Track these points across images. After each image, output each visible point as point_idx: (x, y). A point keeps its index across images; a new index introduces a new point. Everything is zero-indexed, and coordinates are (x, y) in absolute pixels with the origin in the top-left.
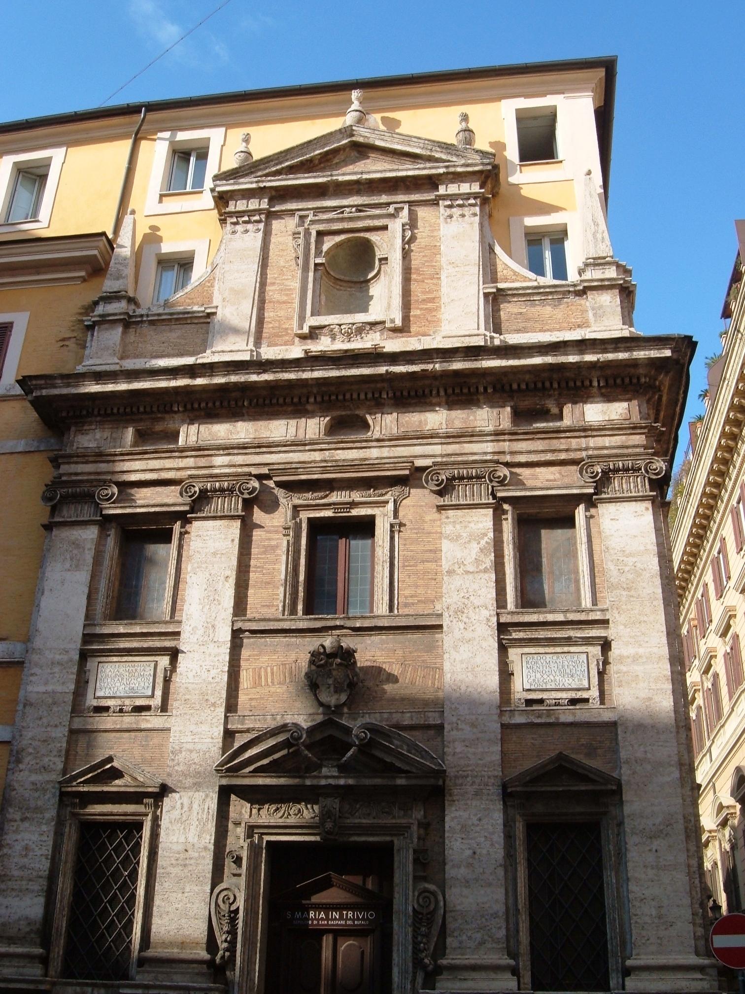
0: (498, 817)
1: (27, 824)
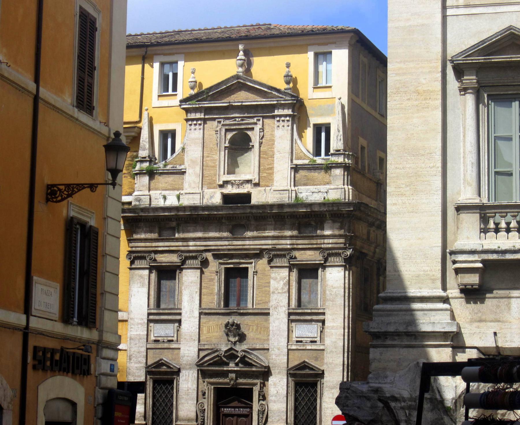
0: (285, 380)
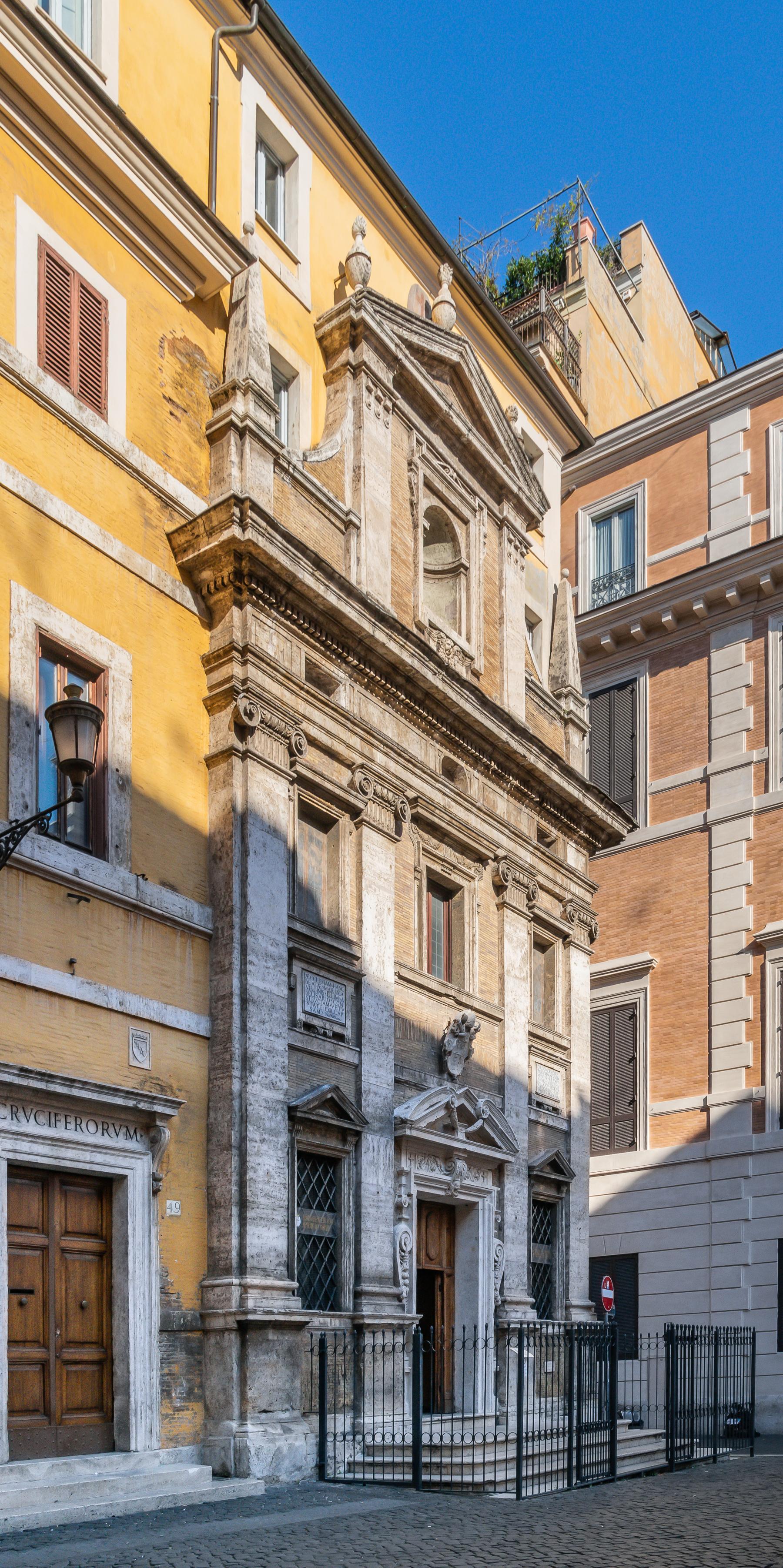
1: (265, 1147)
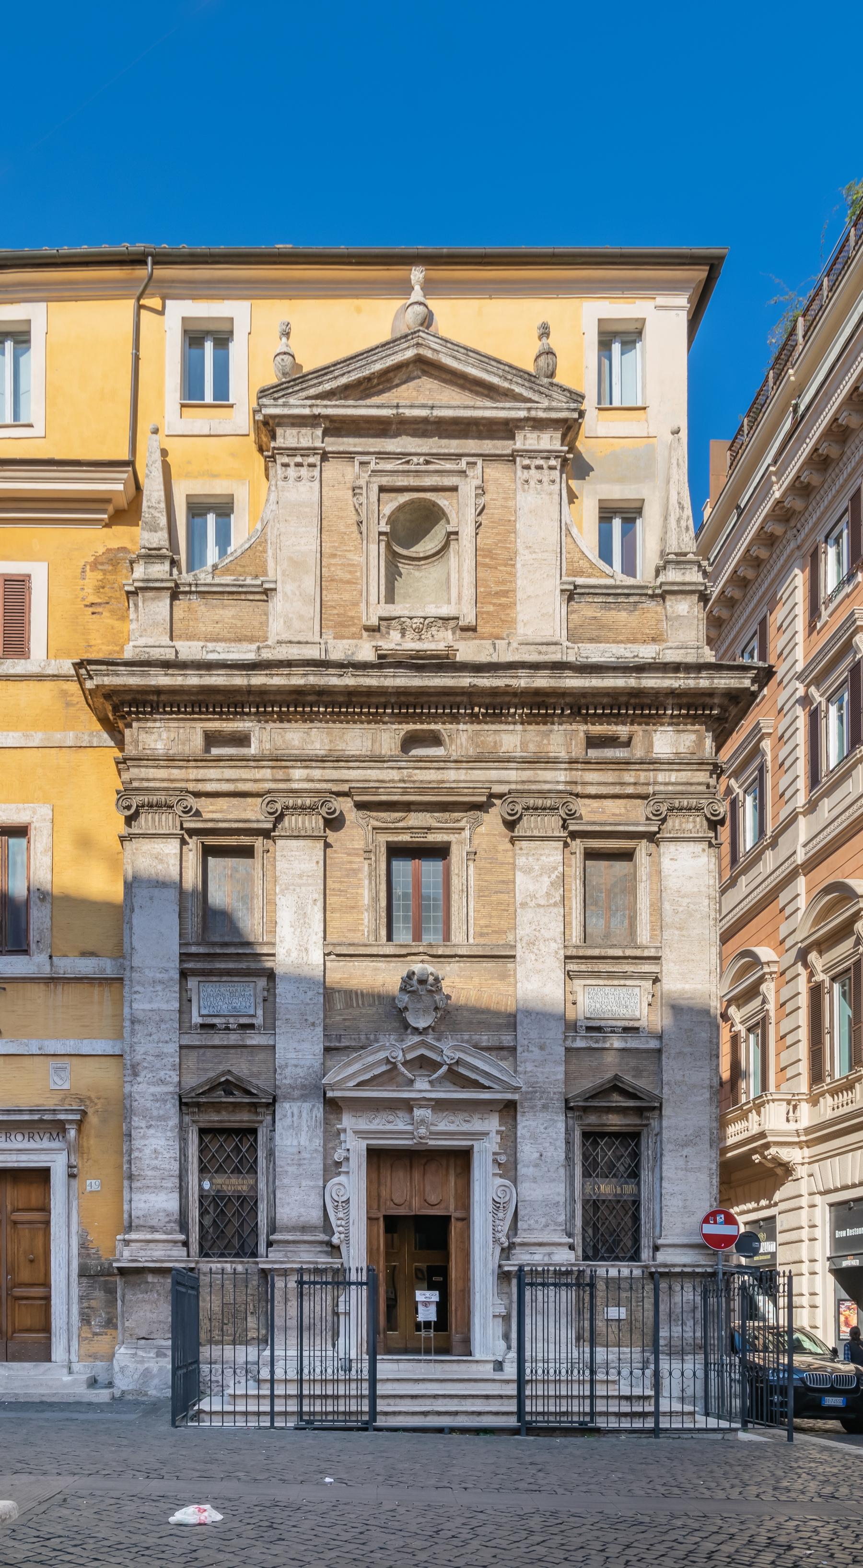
0: (561, 1126)
1: (152, 1131)
